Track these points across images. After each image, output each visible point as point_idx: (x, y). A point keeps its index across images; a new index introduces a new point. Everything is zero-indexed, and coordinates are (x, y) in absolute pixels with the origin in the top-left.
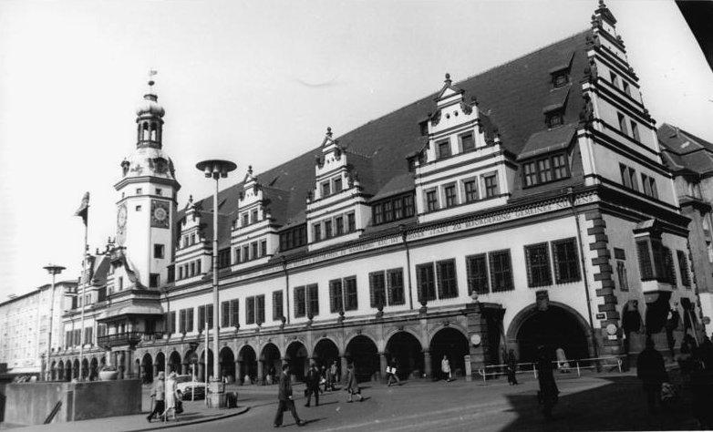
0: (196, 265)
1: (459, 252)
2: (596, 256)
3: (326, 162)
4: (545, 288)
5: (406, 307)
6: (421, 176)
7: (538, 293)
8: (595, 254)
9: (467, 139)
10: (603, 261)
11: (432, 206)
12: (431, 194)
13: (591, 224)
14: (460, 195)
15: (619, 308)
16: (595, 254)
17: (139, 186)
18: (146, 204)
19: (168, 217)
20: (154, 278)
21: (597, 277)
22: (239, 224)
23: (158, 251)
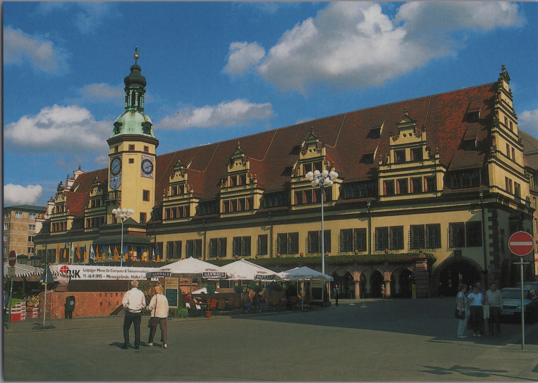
0: (184, 210)
1: (406, 222)
2: (492, 233)
3: (309, 152)
4: (459, 249)
5: (366, 253)
6: (384, 172)
7: (455, 251)
8: (491, 232)
9: (417, 155)
10: (494, 236)
11: (390, 191)
13: (490, 215)
14: (410, 187)
15: (501, 263)
16: (491, 232)
17: (132, 143)
18: (138, 158)
19: (152, 169)
20: (143, 216)
21: (491, 245)
22: (229, 183)
23: (146, 195)
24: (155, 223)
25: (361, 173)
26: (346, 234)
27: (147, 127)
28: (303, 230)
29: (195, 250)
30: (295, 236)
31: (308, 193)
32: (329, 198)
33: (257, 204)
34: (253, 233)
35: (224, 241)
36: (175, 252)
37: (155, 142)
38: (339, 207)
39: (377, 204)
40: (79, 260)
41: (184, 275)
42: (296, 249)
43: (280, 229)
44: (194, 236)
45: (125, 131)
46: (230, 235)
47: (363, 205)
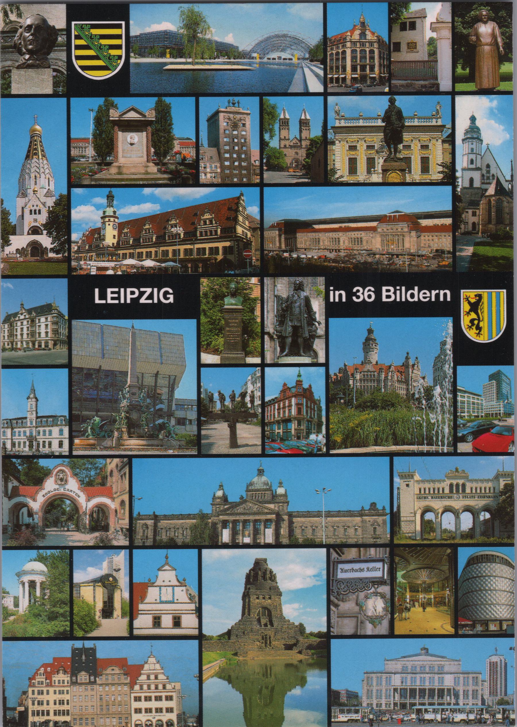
11: (201, 235)
12: (201, 233)
24: (118, 247)
25: (191, 229)
26: (186, 250)
27: (115, 212)
28: (170, 249)
29: (132, 256)
30: (167, 251)
31: (172, 236)
32: (180, 238)
33: (154, 240)
34: (153, 250)
35: (142, 253)
36: (125, 257)
37: (117, 218)
38: (183, 240)
39: (197, 239)
40: (91, 260)
41: (128, 265)
42: (167, 255)
43: (162, 248)
44: (132, 251)
45: (107, 214)
46: (144, 250)
47: (192, 240)
